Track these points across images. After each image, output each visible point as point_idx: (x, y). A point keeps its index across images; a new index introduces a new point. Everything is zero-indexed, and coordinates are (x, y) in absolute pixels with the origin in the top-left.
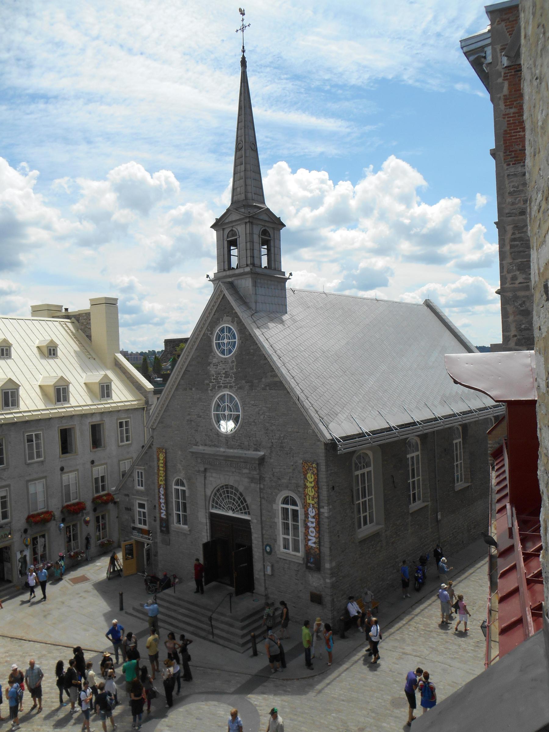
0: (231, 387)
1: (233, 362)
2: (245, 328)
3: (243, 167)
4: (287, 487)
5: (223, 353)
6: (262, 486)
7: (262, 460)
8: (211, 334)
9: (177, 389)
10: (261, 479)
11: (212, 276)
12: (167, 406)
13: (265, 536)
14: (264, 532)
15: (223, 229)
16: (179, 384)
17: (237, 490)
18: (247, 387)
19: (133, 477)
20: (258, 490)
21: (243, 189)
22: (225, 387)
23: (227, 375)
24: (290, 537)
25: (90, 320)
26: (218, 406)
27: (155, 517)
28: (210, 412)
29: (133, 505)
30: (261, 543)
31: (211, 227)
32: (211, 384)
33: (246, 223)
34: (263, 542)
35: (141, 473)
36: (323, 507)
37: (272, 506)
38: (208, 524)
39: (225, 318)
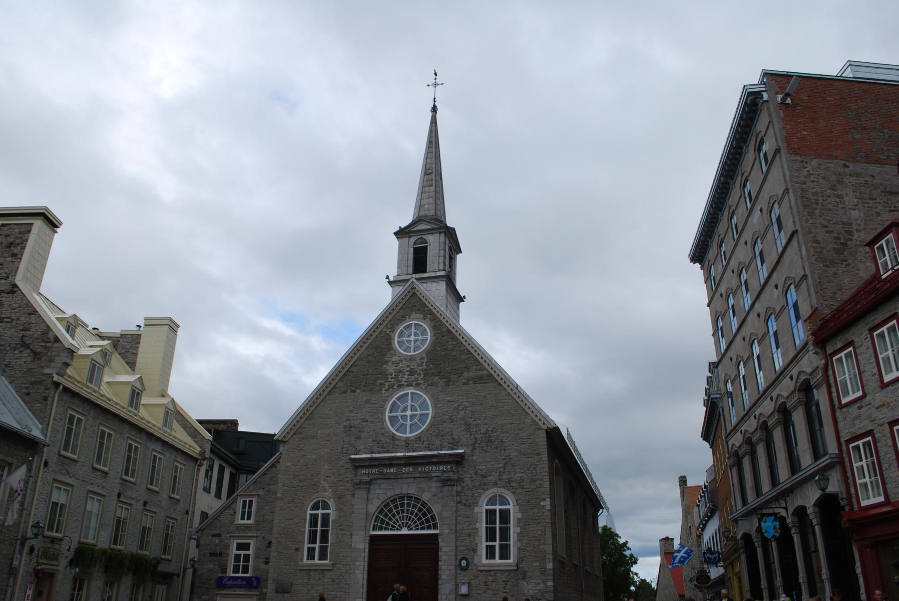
0: (417, 385)
1: (422, 358)
2: (442, 324)
3: (432, 189)
4: (495, 484)
5: (407, 349)
6: (459, 489)
7: (459, 460)
8: (392, 331)
11: (391, 279)
12: (312, 413)
13: (459, 548)
14: (459, 543)
15: (410, 237)
17: (417, 500)
18: (442, 382)
19: (235, 509)
20: (454, 493)
21: (432, 206)
22: (407, 386)
23: (412, 372)
24: (497, 544)
25: (138, 343)
26: (394, 408)
27: (268, 558)
28: (383, 414)
29: (227, 547)
30: (454, 558)
31: (396, 234)
32: (387, 384)
33: (440, 233)
34: (456, 556)
35: (251, 502)
36: (545, 499)
37: (473, 510)
38: (367, 550)
39: (413, 315)
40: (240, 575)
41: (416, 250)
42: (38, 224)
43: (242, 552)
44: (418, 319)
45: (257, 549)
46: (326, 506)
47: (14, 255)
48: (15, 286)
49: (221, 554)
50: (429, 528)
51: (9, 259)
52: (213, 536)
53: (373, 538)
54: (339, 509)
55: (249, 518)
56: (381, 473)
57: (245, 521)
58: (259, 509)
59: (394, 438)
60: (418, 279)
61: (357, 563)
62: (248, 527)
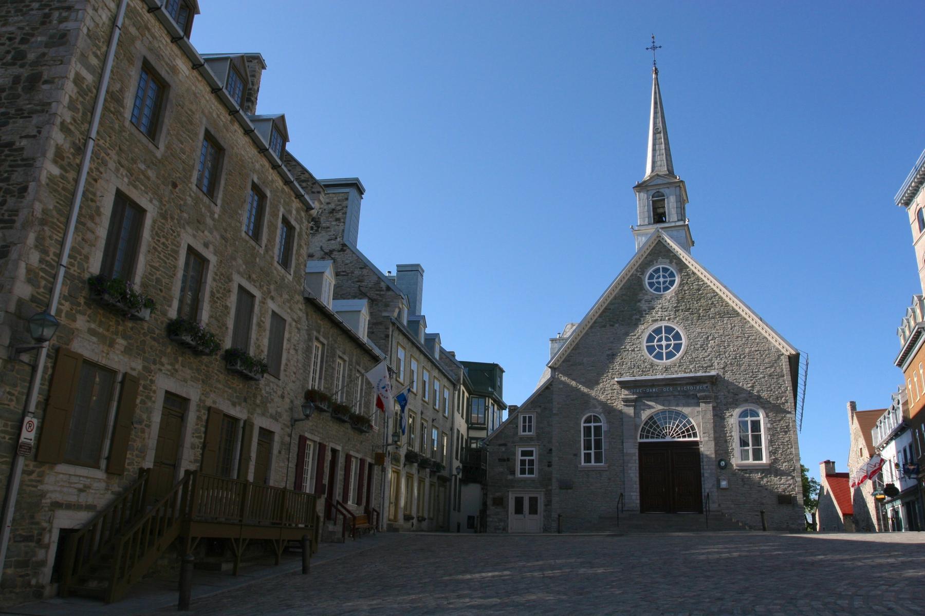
4: (746, 401)
8: (643, 274)
9: (591, 327)
10: (716, 398)
16: (595, 322)
29: (514, 454)
35: (530, 418)
39: (660, 259)
40: (527, 476)
41: (653, 202)
42: (353, 192)
43: (527, 458)
44: (665, 263)
45: (540, 455)
46: (597, 419)
47: (338, 220)
48: (344, 245)
49: (508, 460)
50: (689, 436)
51: (334, 223)
52: (500, 445)
53: (640, 443)
54: (609, 422)
55: (530, 430)
56: (645, 393)
57: (527, 433)
58: (537, 422)
59: (652, 365)
60: (662, 228)
61: (630, 465)
62: (530, 439)
